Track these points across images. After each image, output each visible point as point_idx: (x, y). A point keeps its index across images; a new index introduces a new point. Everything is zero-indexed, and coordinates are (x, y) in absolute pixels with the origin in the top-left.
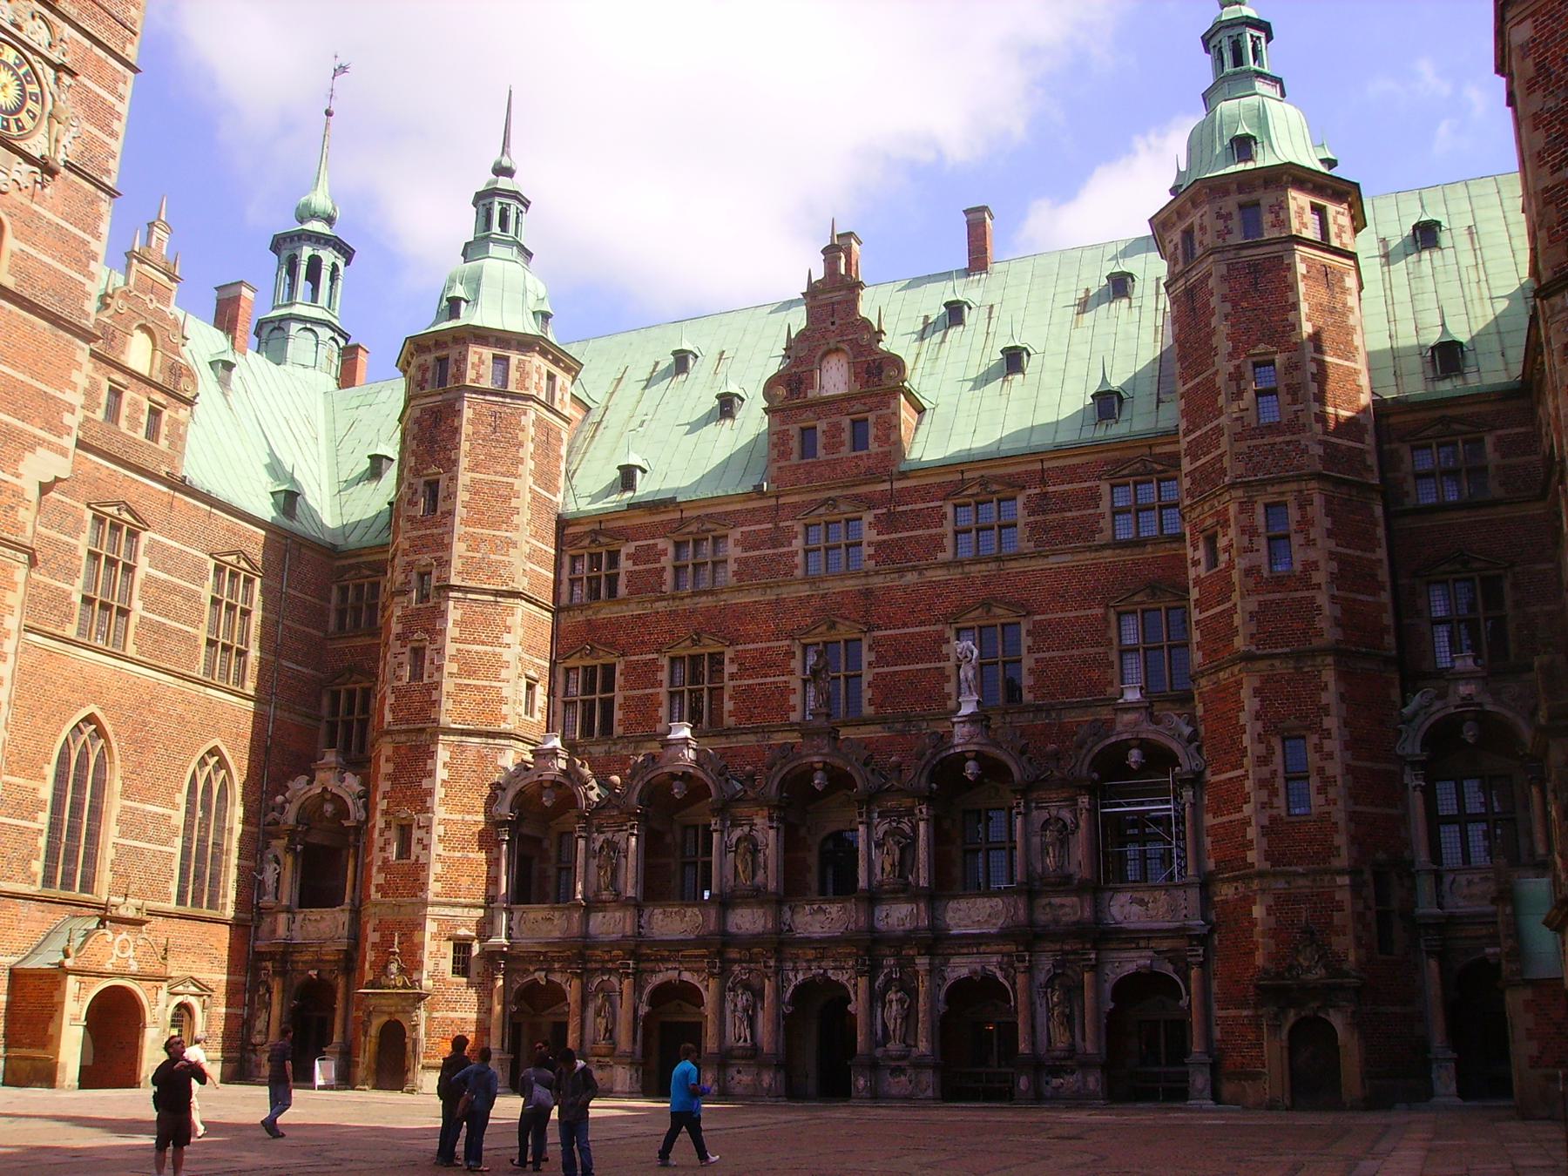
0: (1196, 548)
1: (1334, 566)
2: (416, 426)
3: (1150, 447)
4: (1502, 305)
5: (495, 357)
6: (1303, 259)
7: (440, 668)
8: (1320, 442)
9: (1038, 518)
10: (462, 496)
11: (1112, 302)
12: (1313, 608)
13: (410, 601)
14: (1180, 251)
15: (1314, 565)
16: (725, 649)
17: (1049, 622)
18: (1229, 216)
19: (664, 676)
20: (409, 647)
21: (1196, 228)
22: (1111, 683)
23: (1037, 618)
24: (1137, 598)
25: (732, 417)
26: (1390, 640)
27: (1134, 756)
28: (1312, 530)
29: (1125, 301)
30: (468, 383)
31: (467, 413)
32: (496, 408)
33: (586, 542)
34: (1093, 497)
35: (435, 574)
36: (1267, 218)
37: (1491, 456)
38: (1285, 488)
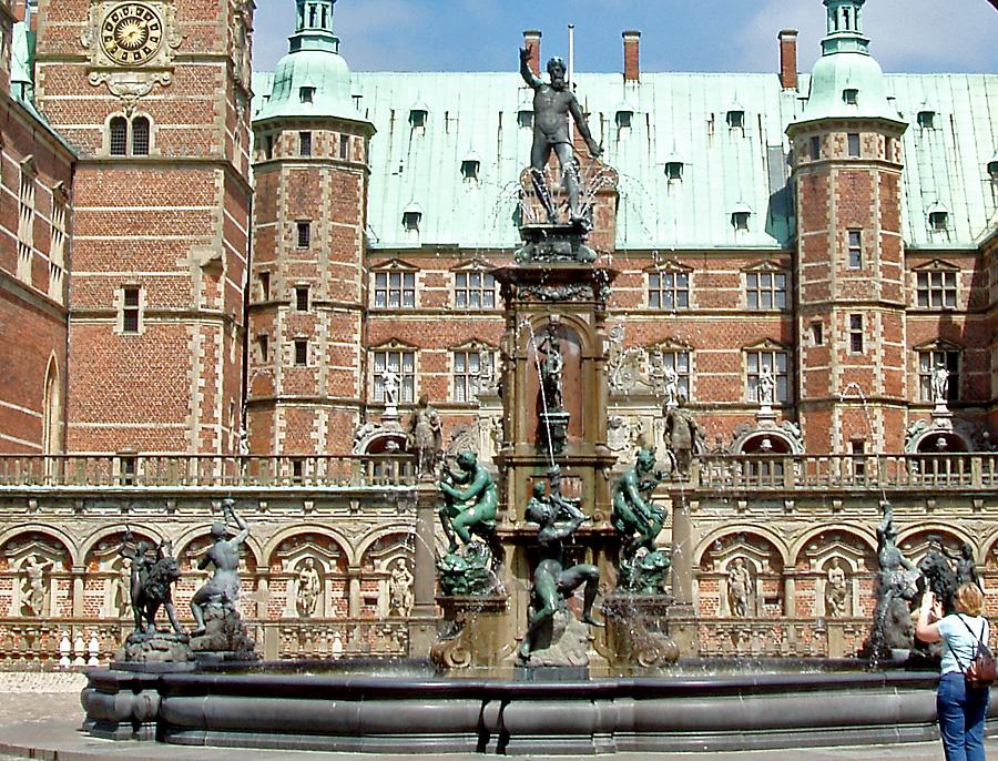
0: (806, 330)
1: (883, 352)
8: (882, 283)
9: (702, 289)
12: (871, 375)
14: (807, 150)
17: (707, 354)
19: (450, 364)
20: (293, 342)
21: (821, 139)
22: (742, 395)
23: (700, 351)
24: (759, 346)
27: (767, 444)
28: (874, 333)
33: (389, 267)
34: (737, 282)
36: (863, 146)
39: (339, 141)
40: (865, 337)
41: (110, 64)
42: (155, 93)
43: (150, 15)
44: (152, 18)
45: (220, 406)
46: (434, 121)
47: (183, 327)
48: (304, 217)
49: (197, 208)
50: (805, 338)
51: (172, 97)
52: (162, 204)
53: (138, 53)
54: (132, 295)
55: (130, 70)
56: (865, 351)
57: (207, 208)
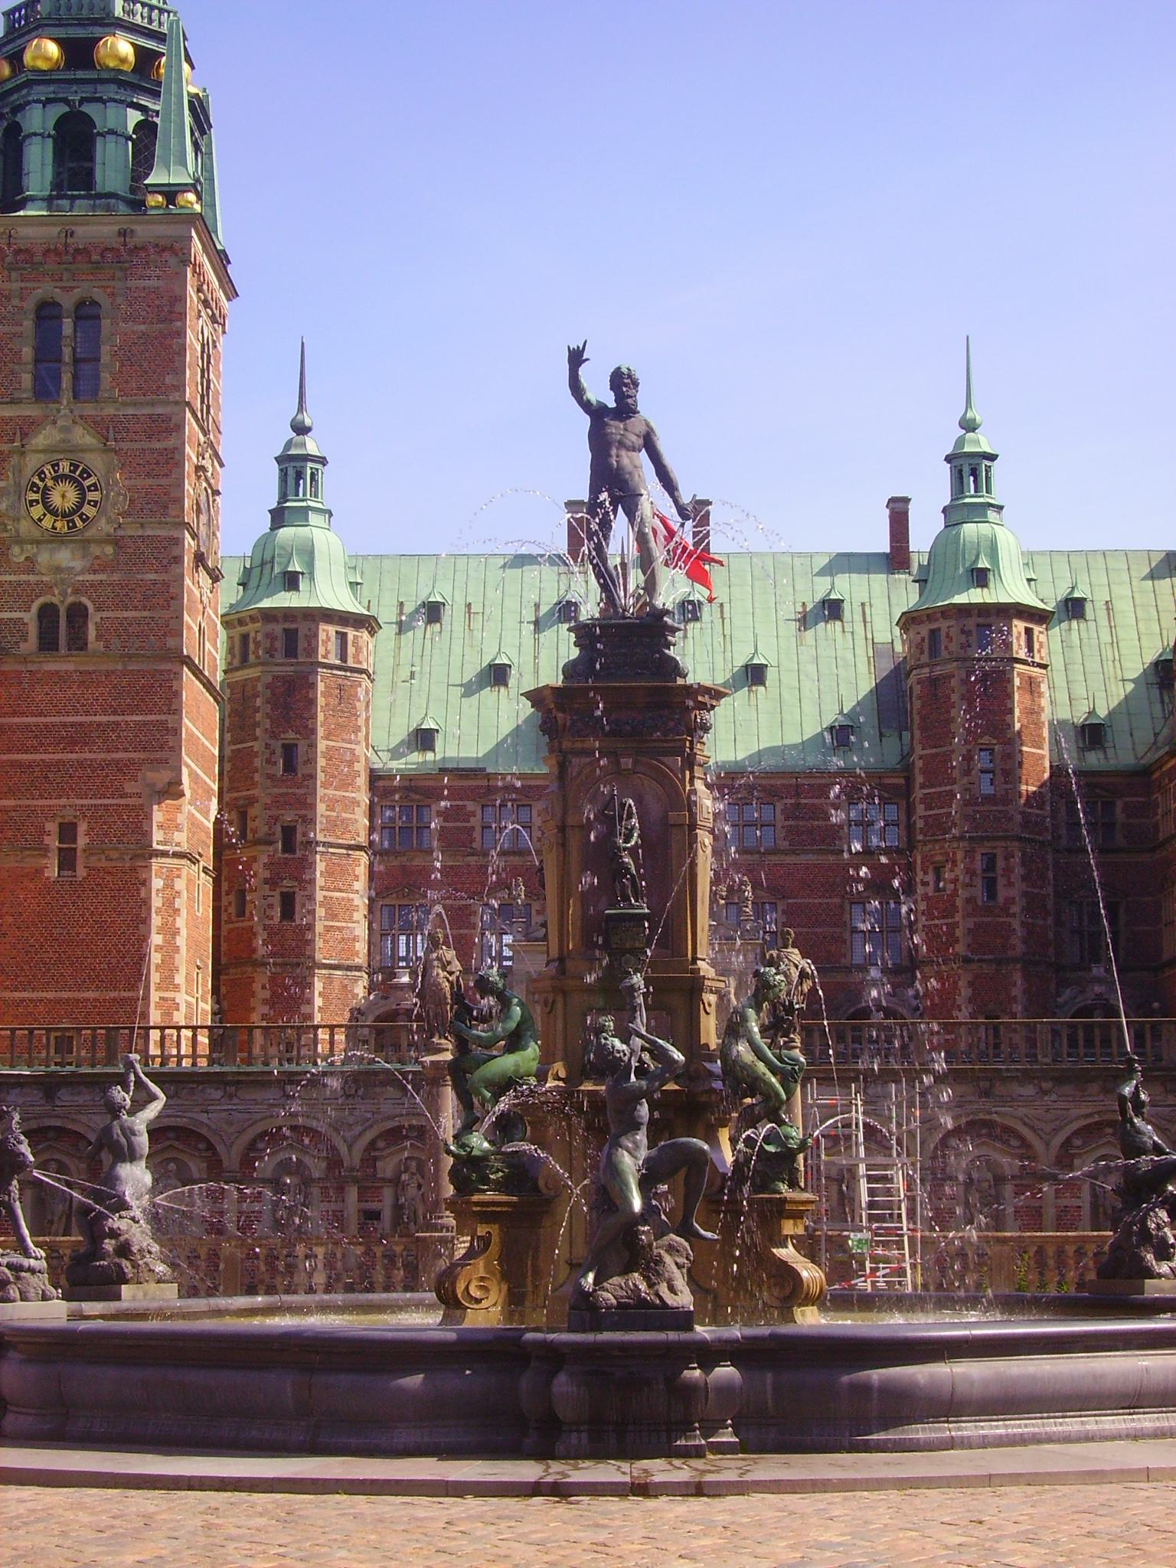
1: (1024, 901)
2: (269, 692)
3: (880, 778)
4: (1130, 687)
5: (337, 632)
6: (1019, 674)
7: (313, 912)
8: (1020, 813)
10: (321, 762)
11: (827, 622)
13: (276, 851)
15: (1010, 901)
16: (532, 902)
18: (968, 633)
20: (278, 891)
22: (844, 956)
23: (790, 901)
25: (506, 685)
26: (1051, 951)
29: (838, 624)
30: (321, 660)
31: (321, 687)
32: (340, 681)
35: (300, 829)
37: (1120, 816)
38: (998, 843)
39: (333, 639)
40: (1001, 881)
41: (36, 533)
42: (95, 572)
43: (87, 473)
44: (89, 476)
45: (183, 971)
46: (453, 616)
47: (133, 869)
48: (291, 735)
49: (149, 718)
50: (925, 884)
51: (116, 577)
52: (105, 713)
53: (73, 521)
54: (68, 832)
55: (62, 542)
56: (1000, 899)
57: (163, 717)
